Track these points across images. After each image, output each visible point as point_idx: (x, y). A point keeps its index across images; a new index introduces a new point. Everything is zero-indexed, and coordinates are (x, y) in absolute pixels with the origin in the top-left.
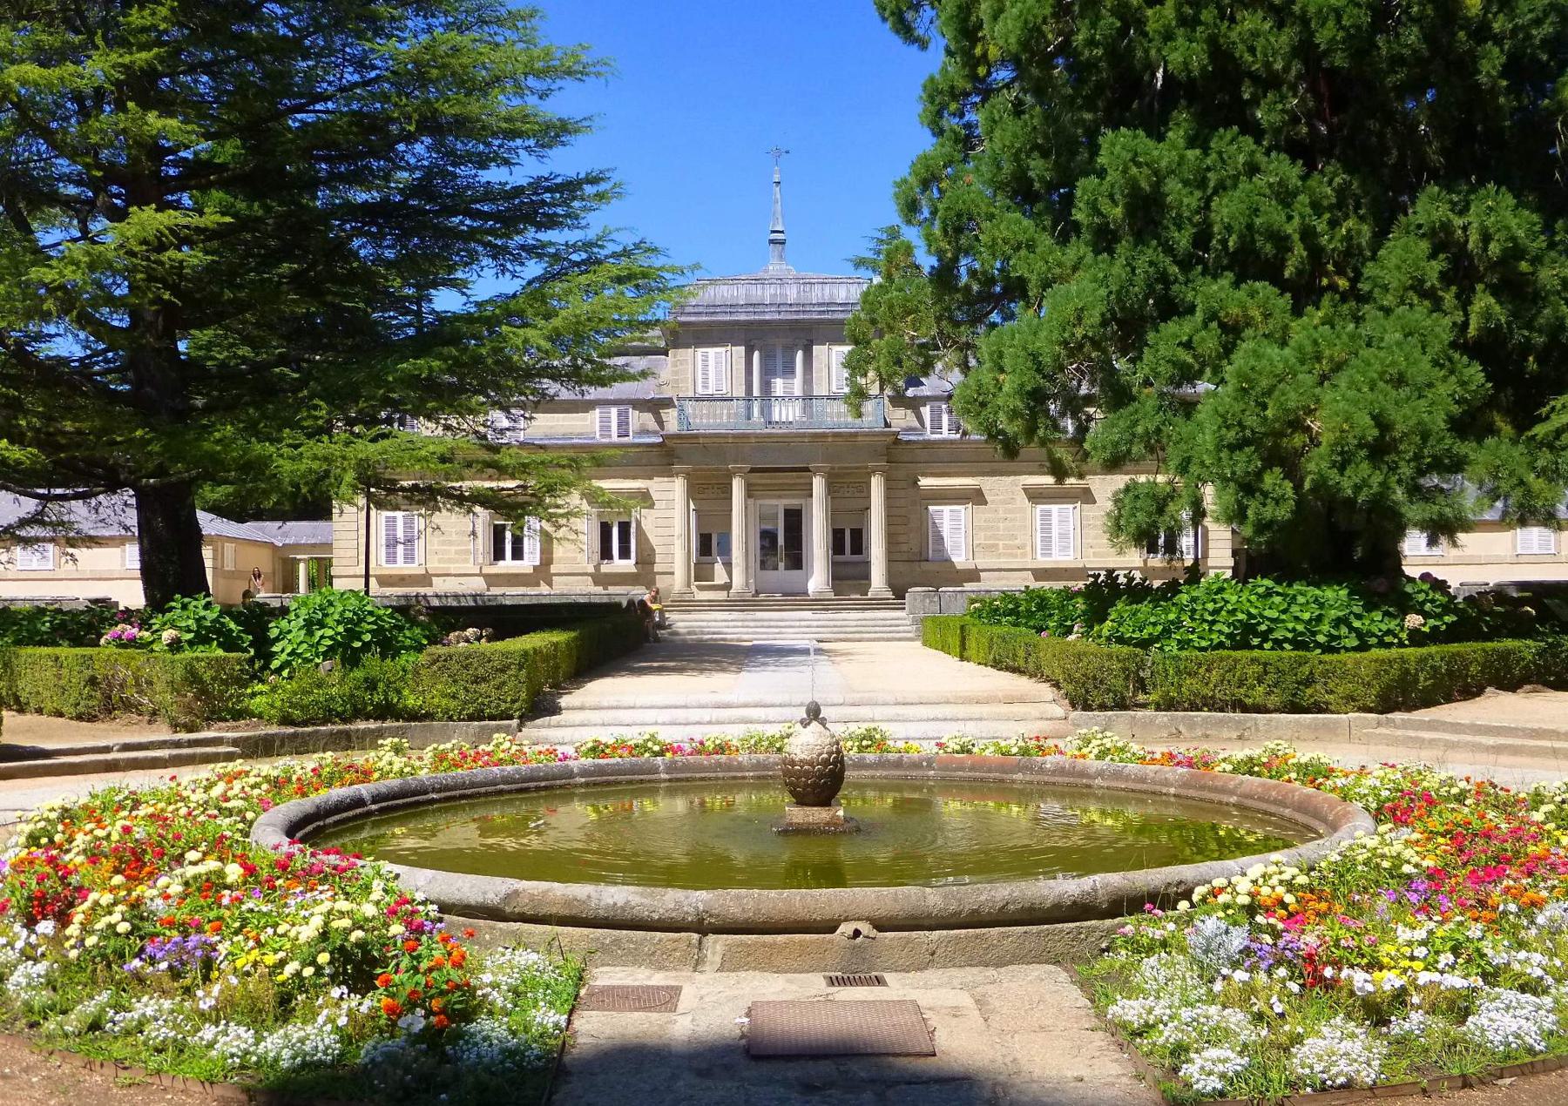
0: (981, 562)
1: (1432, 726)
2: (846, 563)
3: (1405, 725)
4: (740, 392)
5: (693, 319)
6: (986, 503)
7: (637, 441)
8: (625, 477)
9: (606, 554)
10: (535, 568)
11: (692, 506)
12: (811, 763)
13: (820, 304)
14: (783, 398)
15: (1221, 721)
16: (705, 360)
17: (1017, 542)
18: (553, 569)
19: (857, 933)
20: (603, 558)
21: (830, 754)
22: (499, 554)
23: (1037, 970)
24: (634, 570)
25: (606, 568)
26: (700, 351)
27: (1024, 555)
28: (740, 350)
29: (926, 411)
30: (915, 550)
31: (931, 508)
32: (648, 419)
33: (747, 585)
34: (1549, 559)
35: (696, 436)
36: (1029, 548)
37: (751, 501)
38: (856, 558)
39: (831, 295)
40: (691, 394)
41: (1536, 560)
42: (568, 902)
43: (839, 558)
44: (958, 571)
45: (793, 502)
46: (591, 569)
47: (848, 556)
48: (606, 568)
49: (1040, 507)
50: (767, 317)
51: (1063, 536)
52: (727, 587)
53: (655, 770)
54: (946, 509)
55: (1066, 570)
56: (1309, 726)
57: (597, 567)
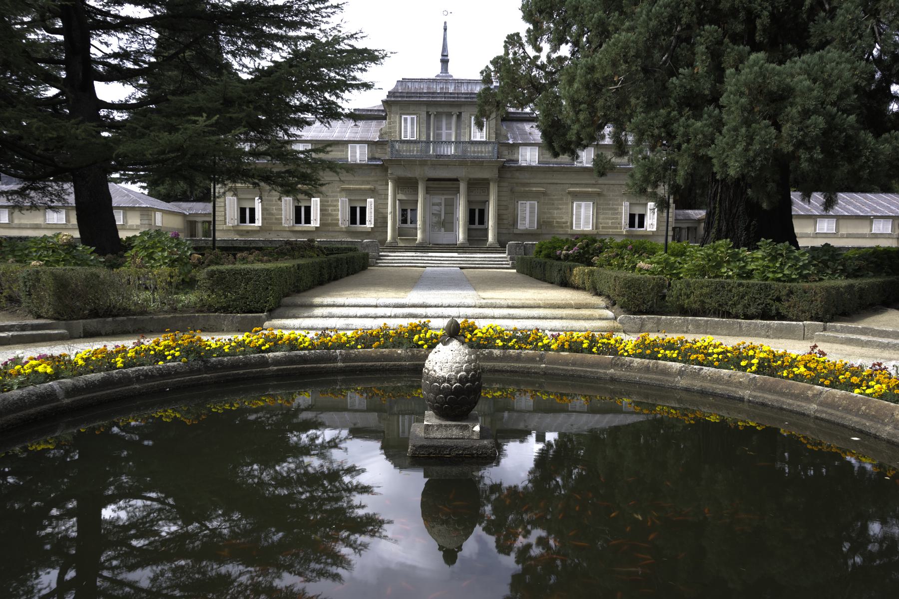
1: (864, 331)
3: (842, 330)
12: (448, 380)
14: (445, 142)
15: (717, 323)
17: (563, 220)
21: (467, 371)
34: (832, 236)
38: (481, 227)
39: (471, 90)
41: (825, 236)
53: (334, 359)
56: (776, 329)
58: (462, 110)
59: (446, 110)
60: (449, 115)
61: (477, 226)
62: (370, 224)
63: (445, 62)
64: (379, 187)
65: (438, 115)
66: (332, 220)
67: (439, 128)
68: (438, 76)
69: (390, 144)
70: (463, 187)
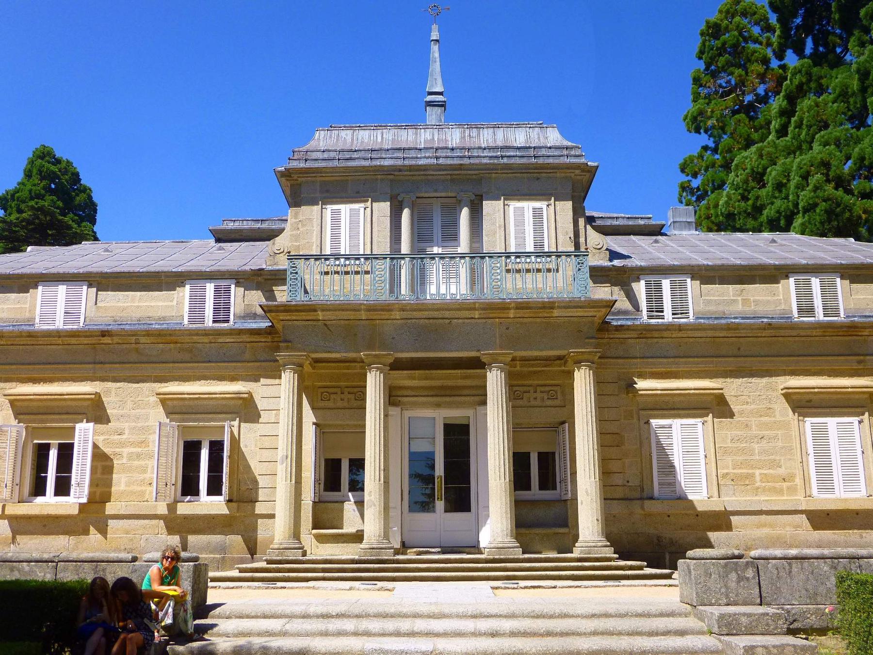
0: (731, 500)
2: (533, 503)
4: (383, 246)
5: (323, 164)
6: (731, 415)
7: (237, 326)
8: (221, 378)
9: (189, 487)
10: (82, 506)
11: (309, 417)
13: (490, 149)
16: (336, 219)
17: (782, 471)
18: (111, 508)
20: (185, 493)
22: (39, 489)
24: (225, 511)
25: (185, 508)
26: (330, 208)
27: (792, 490)
28: (384, 208)
29: (640, 288)
30: (635, 482)
31: (654, 422)
32: (256, 298)
33: (386, 536)
35: (311, 308)
36: (798, 481)
37: (394, 411)
38: (547, 494)
43: (524, 494)
44: (698, 514)
45: (455, 414)
46: (162, 509)
47: (535, 492)
48: (185, 508)
49: (809, 421)
50: (421, 162)
51: (848, 463)
52: (358, 537)
54: (677, 424)
55: (857, 513)
57: (172, 507)
66: (128, 484)
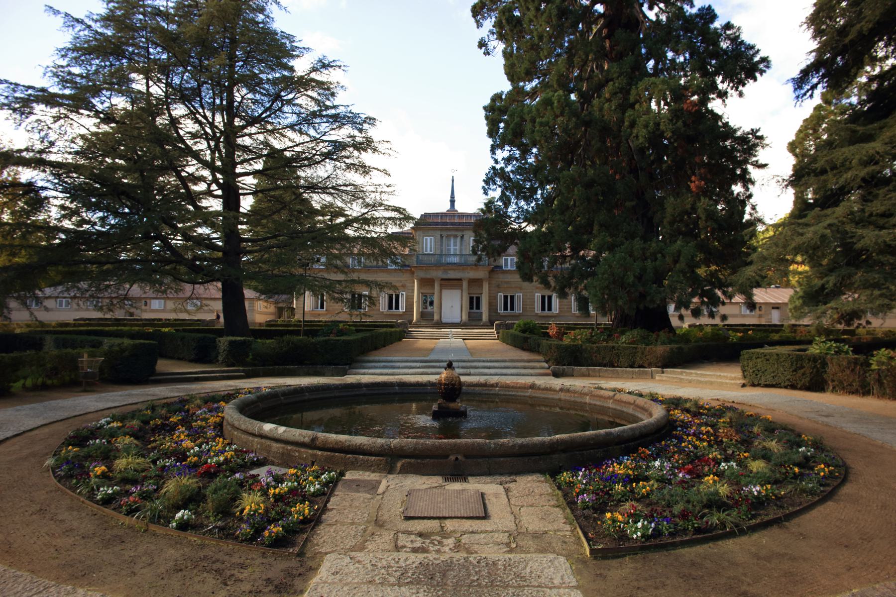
19: (457, 459)
23: (535, 477)
38: (478, 311)
40: (421, 253)
42: (337, 442)
58: (464, 233)
59: (454, 233)
60: (456, 237)
61: (475, 310)
62: (402, 309)
63: (452, 202)
64: (408, 285)
65: (448, 237)
67: (449, 245)
68: (448, 211)
69: (415, 256)
70: (465, 284)
